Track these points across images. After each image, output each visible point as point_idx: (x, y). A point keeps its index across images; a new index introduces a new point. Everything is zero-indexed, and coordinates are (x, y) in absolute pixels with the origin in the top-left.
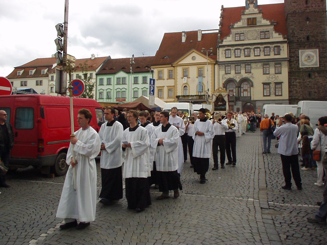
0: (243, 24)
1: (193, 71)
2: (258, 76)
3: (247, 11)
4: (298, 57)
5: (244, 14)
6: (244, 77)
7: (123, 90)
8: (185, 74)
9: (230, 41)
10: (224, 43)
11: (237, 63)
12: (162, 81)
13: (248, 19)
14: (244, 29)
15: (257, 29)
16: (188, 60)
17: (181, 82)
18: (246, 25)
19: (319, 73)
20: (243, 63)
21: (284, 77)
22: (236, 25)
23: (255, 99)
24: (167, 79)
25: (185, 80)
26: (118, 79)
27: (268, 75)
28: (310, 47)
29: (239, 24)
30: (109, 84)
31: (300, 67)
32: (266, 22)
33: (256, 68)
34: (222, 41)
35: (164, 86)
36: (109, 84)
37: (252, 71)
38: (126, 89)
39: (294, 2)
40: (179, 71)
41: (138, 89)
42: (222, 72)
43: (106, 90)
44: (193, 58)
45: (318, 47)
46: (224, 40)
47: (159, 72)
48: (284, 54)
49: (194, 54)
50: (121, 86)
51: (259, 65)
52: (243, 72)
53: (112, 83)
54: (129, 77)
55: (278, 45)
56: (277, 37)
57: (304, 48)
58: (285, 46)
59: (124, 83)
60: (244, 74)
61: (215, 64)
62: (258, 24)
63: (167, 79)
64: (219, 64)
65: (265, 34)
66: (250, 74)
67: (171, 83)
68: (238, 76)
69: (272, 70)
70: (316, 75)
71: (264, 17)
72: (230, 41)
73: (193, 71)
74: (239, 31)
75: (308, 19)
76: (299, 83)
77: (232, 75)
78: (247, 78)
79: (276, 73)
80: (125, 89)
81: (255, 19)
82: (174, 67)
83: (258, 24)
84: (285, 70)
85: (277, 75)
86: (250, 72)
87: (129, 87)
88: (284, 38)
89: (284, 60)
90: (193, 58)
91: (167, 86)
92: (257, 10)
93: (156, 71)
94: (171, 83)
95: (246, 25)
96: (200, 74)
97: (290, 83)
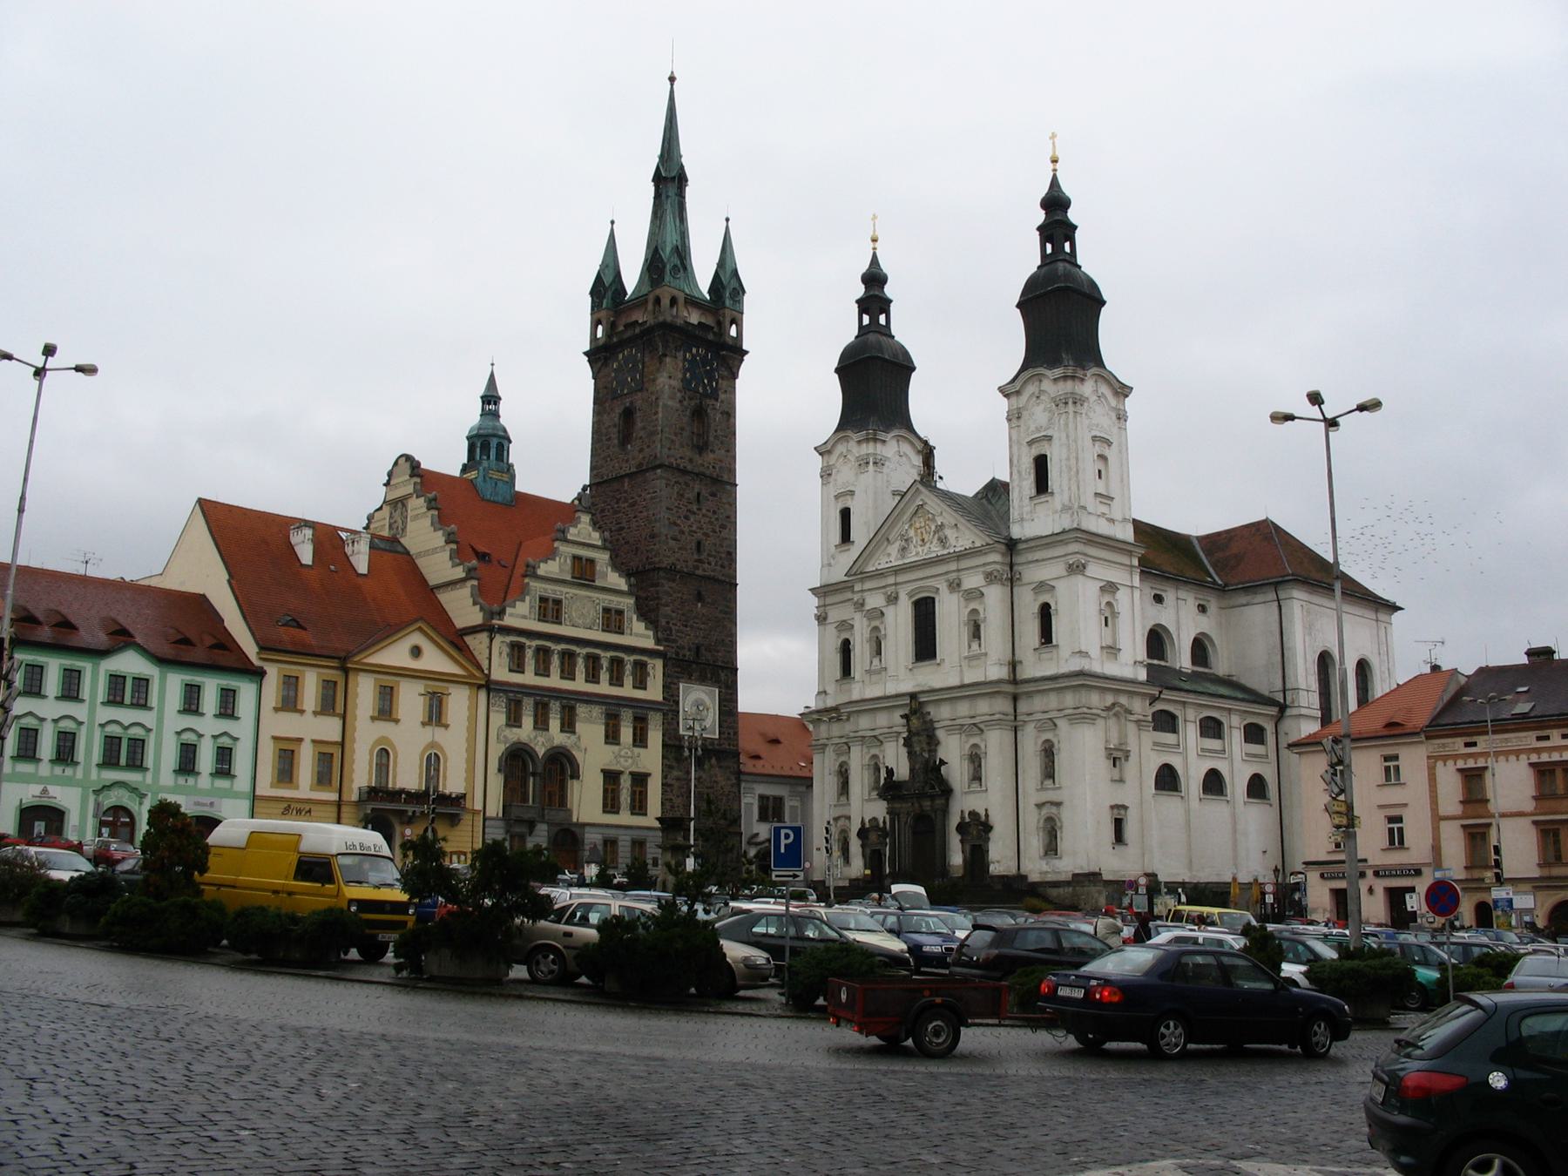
0: (561, 570)
1: (411, 699)
2: (593, 749)
3: (572, 533)
4: (677, 703)
5: (566, 541)
6: (556, 742)
7: (137, 732)
8: (386, 710)
9: (524, 617)
10: (508, 621)
11: (543, 700)
12: (296, 716)
13: (576, 558)
14: (565, 590)
15: (595, 595)
16: (395, 655)
17: (366, 734)
18: (569, 578)
19: (718, 759)
20: (557, 698)
21: (651, 759)
22: (543, 569)
23: (584, 819)
24: (315, 713)
25: (384, 728)
26: (116, 681)
27: (616, 748)
28: (702, 680)
29: (548, 568)
30: (70, 692)
31: (681, 732)
32: (616, 580)
33: (589, 720)
34: (501, 613)
35: (300, 740)
36: (70, 692)
37: (579, 727)
38: (149, 730)
39: (674, 539)
40: (365, 691)
41: (201, 736)
42: (499, 718)
43: (55, 721)
44: (416, 652)
45: (716, 681)
46: (509, 610)
47: (291, 685)
48: (654, 691)
49: (417, 639)
50: (127, 716)
51: (597, 711)
52: (555, 724)
53: (85, 693)
54: (163, 680)
55: (644, 658)
56: (639, 635)
57: (690, 679)
58: (659, 663)
59: (141, 704)
60: (556, 734)
61: (479, 687)
62: (597, 583)
63: (315, 713)
64: (489, 691)
65: (612, 619)
66: (573, 738)
67: (330, 729)
68: (540, 739)
69: (626, 733)
70: (713, 761)
71: (616, 565)
72: (524, 617)
73: (411, 699)
74: (551, 590)
75: (699, 597)
76: (678, 779)
77: (526, 731)
78: (564, 748)
79: (635, 745)
80: (143, 726)
81: (591, 562)
82: (346, 671)
83: (597, 583)
84: (655, 737)
85: (637, 750)
86: (574, 732)
87: (160, 720)
88: (658, 642)
89: (651, 705)
90: (416, 652)
91: (314, 741)
92: (596, 535)
93: (273, 673)
94: (330, 729)
95: (569, 578)
96: (435, 714)
97: (664, 777)
